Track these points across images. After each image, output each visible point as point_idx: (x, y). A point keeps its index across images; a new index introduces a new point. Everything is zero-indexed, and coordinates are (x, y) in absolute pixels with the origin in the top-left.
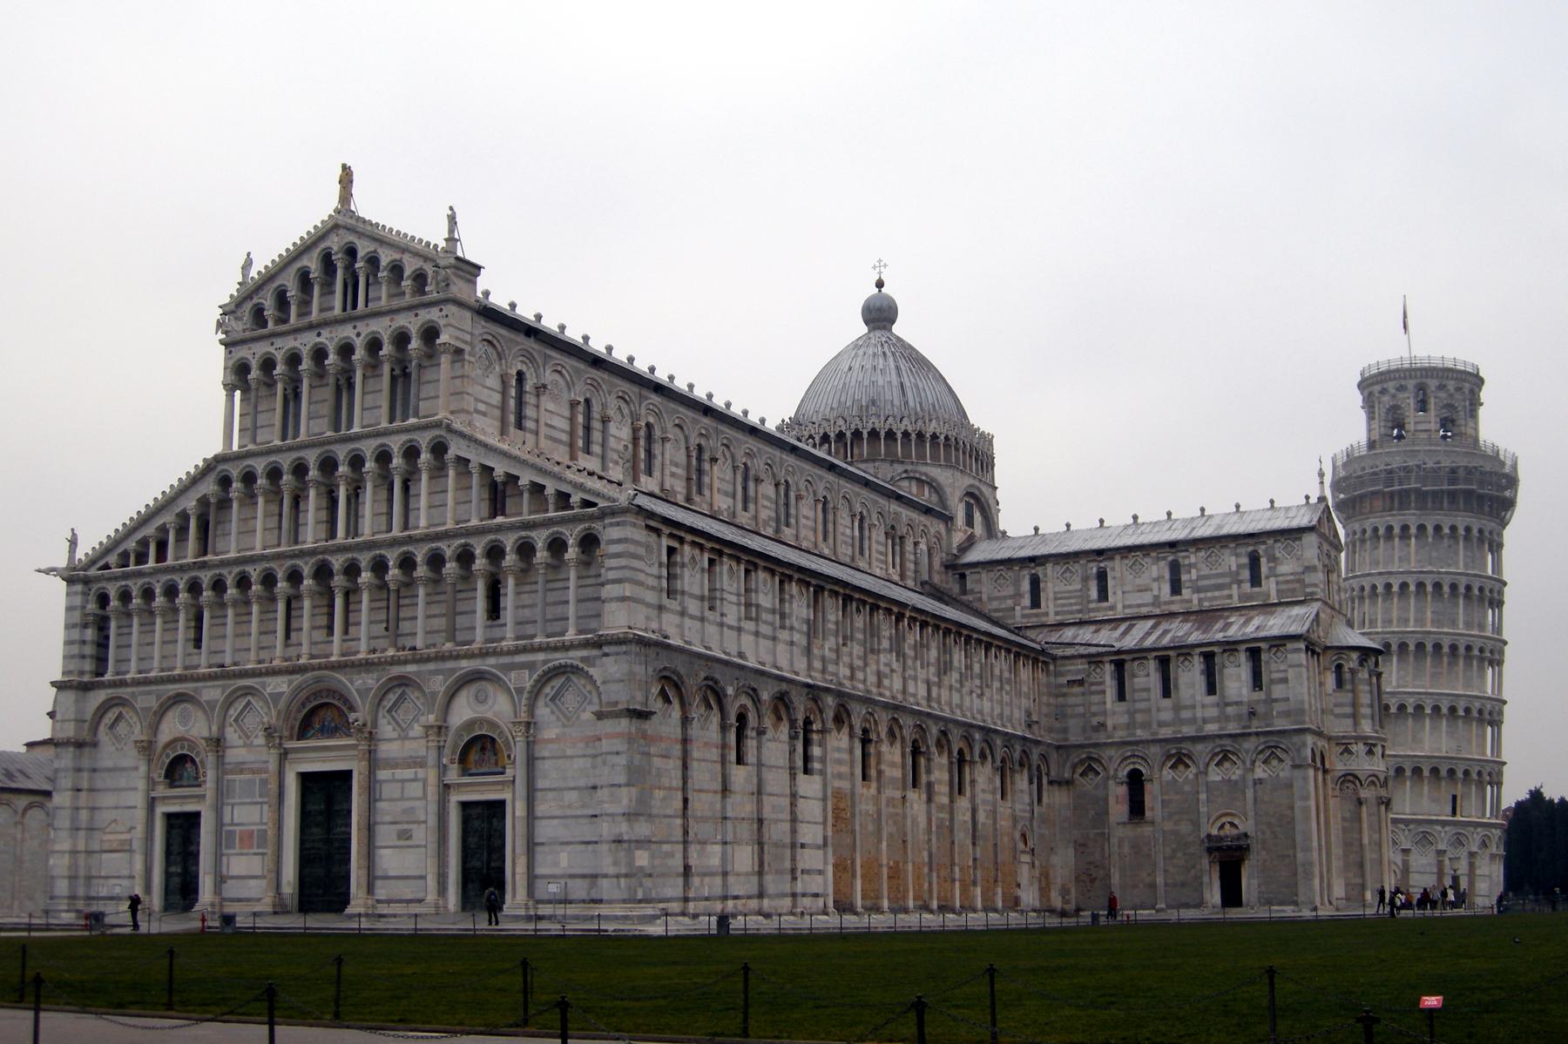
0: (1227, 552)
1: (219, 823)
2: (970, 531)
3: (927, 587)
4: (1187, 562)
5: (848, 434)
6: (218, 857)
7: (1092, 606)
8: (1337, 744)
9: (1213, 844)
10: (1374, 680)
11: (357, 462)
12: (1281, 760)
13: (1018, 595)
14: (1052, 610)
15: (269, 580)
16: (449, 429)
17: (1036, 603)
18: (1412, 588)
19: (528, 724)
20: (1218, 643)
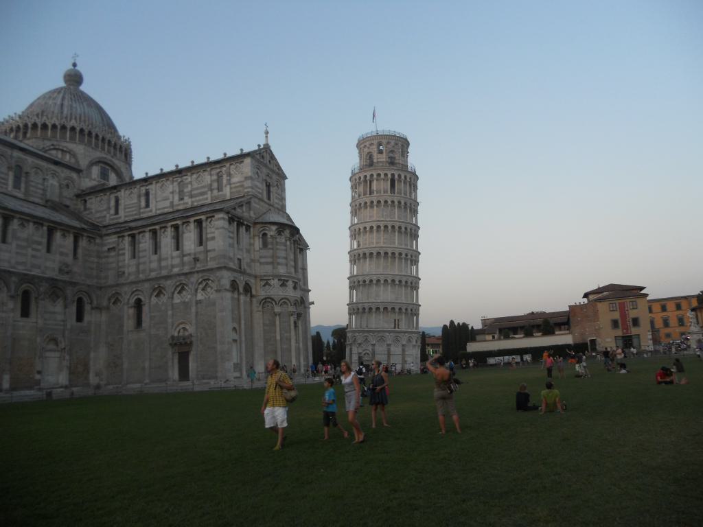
0: (206, 173)
2: (103, 182)
3: (49, 203)
4: (187, 181)
7: (142, 211)
8: (261, 280)
9: (175, 342)
10: (288, 243)
12: (212, 288)
13: (109, 208)
17: (117, 212)
18: (375, 228)
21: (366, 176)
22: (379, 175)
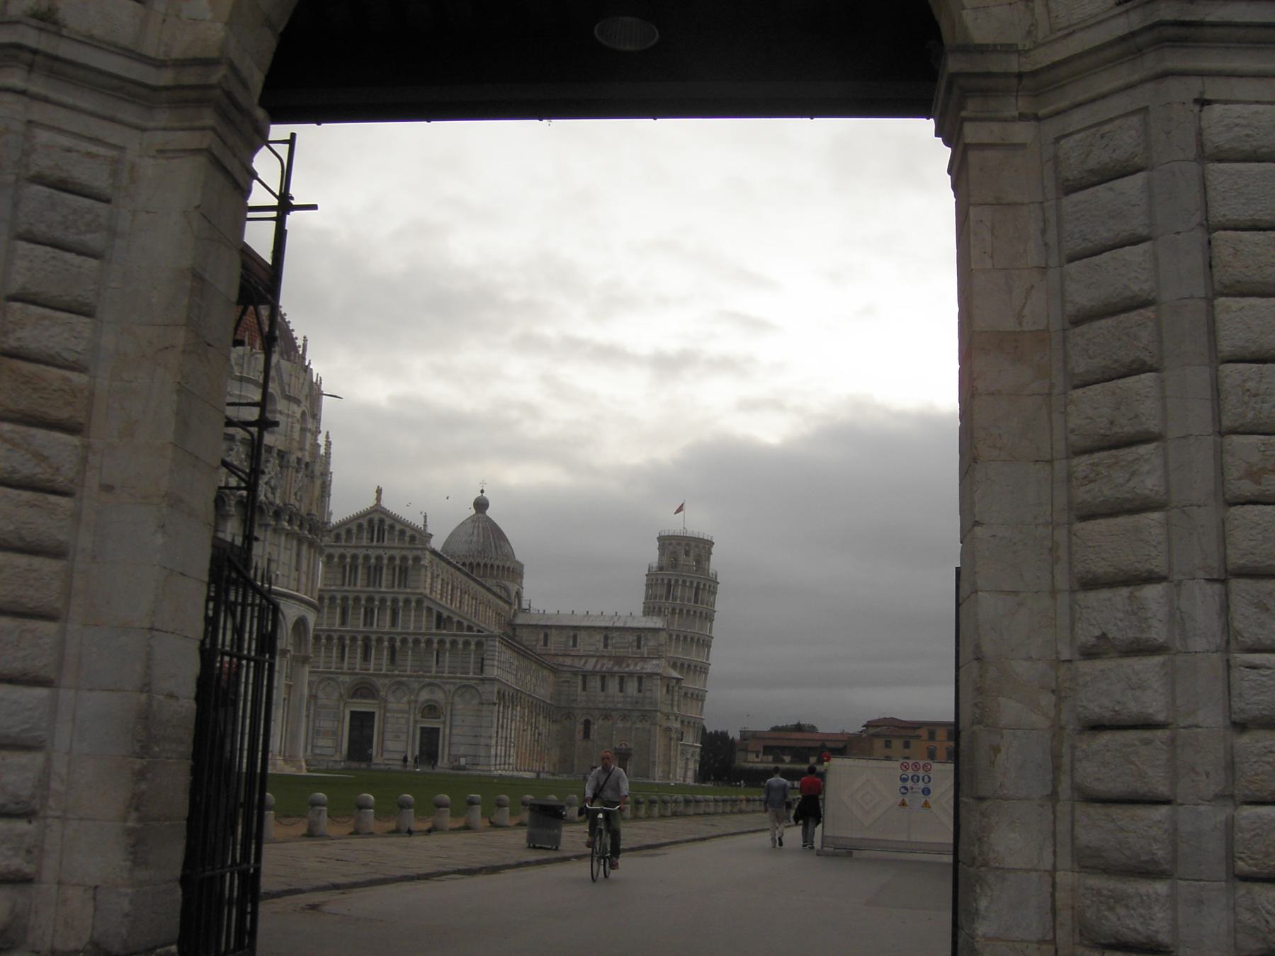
1: (314, 726)
5: (475, 564)
6: (313, 738)
7: (571, 649)
11: (383, 601)
14: (553, 648)
15: (341, 639)
16: (425, 596)
17: (546, 644)
19: (452, 703)
20: (626, 673)
21: (670, 580)
22: (684, 582)
